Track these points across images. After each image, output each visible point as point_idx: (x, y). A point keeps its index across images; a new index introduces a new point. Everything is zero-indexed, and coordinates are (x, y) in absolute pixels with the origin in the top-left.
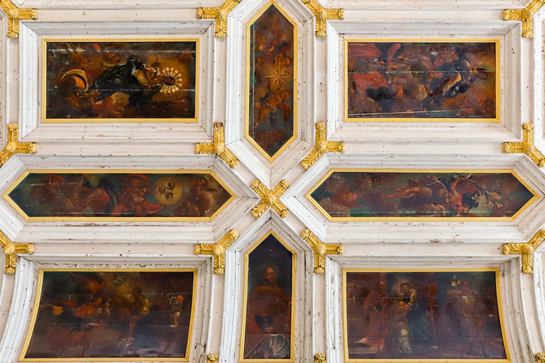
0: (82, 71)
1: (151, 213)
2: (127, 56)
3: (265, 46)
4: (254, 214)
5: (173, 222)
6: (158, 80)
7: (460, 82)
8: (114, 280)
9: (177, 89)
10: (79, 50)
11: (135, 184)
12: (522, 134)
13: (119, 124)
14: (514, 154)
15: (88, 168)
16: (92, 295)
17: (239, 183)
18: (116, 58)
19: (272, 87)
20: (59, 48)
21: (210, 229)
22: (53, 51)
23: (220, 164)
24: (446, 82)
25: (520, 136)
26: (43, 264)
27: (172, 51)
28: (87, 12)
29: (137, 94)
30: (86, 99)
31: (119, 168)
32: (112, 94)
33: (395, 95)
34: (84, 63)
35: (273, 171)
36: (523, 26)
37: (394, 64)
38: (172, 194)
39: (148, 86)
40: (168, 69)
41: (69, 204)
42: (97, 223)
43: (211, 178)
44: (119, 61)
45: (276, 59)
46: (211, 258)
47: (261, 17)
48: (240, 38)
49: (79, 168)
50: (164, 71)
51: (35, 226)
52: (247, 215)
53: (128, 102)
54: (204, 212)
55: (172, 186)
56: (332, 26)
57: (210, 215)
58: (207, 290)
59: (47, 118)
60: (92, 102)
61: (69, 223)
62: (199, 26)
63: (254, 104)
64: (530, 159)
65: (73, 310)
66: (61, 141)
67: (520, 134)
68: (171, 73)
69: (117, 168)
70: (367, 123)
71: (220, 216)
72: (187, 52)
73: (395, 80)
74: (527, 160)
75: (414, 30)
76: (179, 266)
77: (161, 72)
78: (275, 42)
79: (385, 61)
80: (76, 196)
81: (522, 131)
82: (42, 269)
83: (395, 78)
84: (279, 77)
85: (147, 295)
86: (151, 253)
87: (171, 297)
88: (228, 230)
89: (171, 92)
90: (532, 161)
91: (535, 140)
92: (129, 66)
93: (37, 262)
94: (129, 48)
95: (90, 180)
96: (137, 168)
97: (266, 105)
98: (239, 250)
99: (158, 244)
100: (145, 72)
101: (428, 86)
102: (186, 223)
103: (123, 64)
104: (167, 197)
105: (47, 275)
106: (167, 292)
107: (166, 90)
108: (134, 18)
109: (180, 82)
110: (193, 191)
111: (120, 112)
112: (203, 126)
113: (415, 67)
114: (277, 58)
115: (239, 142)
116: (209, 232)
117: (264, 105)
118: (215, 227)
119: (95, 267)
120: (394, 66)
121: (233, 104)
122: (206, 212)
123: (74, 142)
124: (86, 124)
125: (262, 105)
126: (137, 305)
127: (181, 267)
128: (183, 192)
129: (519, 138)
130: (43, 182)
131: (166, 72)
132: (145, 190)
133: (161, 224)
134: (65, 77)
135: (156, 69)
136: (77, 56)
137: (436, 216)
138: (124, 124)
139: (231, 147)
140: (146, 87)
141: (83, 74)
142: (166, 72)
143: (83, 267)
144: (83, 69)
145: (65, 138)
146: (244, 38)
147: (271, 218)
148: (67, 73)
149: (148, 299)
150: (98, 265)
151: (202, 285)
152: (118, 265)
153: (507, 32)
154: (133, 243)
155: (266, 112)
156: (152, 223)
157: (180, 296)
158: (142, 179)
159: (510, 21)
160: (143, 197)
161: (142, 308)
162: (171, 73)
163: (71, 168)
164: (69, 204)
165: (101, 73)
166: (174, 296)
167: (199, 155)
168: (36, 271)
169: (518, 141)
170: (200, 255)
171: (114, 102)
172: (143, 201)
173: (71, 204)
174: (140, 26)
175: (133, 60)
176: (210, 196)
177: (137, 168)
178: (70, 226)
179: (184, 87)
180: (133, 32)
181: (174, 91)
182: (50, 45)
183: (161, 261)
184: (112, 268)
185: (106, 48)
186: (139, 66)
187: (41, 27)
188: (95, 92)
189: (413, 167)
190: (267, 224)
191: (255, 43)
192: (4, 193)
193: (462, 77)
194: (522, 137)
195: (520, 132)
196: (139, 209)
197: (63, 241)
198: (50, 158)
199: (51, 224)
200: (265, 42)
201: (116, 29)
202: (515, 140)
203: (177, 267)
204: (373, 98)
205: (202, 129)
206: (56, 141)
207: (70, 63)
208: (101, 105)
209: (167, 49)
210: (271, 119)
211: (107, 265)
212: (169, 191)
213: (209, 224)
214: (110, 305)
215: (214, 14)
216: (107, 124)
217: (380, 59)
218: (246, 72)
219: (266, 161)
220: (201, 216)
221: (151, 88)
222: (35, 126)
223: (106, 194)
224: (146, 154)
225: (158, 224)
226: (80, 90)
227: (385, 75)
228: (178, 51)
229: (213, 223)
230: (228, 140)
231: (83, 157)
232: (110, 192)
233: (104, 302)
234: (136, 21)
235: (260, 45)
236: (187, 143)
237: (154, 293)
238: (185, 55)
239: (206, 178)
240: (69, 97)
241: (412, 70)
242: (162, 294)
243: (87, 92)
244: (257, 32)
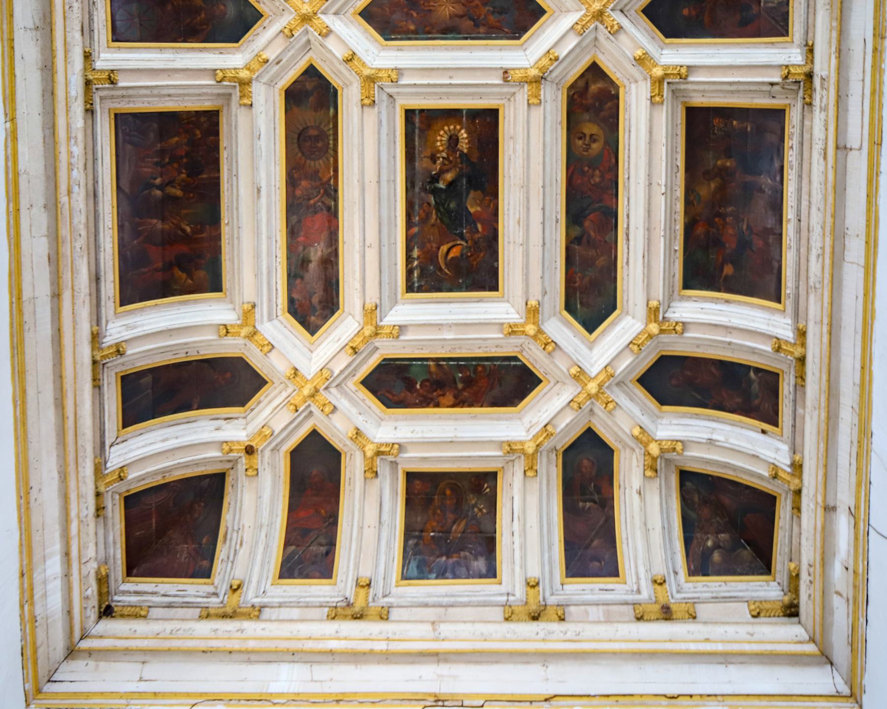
0: (441, 250)
1: (613, 161)
2: (423, 194)
3: (410, 22)
4: (616, 31)
5: (624, 133)
6: (452, 155)
9: (463, 131)
10: (416, 253)
11: (579, 181)
13: (506, 202)
15: (558, 239)
16: (711, 229)
17: (578, 50)
18: (425, 208)
19: (461, 13)
20: (413, 278)
21: (633, 86)
22: (416, 285)
23: (554, 75)
26: (673, 292)
27: (417, 139)
28: (368, 243)
29: (469, 182)
30: (476, 243)
31: (559, 200)
32: (470, 212)
34: (432, 247)
35: (564, 9)
38: (592, 135)
39: (459, 168)
40: (439, 144)
41: (601, 262)
42: (625, 226)
43: (572, 87)
44: (429, 204)
45: (426, 8)
46: (668, 83)
47: (375, 28)
48: (400, 54)
49: (558, 249)
50: (441, 148)
51: (627, 301)
52: (616, 39)
53: (479, 192)
54: (614, 95)
55: (581, 135)
57: (617, 88)
58: (706, 87)
59: (497, 290)
60: (479, 235)
61: (625, 260)
62: (385, 104)
63: (482, 34)
65: (728, 251)
66: (525, 271)
68: (443, 139)
69: (559, 203)
71: (618, 75)
72: (417, 120)
77: (443, 151)
78: (405, 10)
80: (592, 253)
84: (448, 5)
85: (712, 163)
87: (715, 134)
88: (634, 63)
89: (466, 138)
92: (435, 192)
94: (413, 192)
95: (573, 236)
96: (559, 180)
97: (483, 19)
98: (660, 50)
99: (650, 149)
100: (442, 172)
102: (627, 117)
103: (433, 199)
104: (595, 141)
105: (686, 286)
107: (464, 146)
108: (374, 185)
109: (455, 127)
110: (587, 109)
111: (490, 201)
112: (508, 97)
114: (425, 6)
115: (528, 52)
116: (637, 88)
117: (484, 22)
118: (631, 80)
119: (678, 227)
121: (480, 60)
122: (613, 92)
123: (527, 255)
124: (506, 243)
125: (484, 25)
126: (723, 174)
127: (679, 121)
128: (590, 121)
130: (576, 293)
131: (442, 145)
132: (586, 168)
133: (627, 147)
134: (448, 270)
135: (439, 158)
136: (422, 256)
138: (506, 196)
139: (533, 60)
140: (461, 169)
141: (444, 248)
142: (442, 145)
143: (677, 243)
144: (439, 248)
145: (521, 266)
146: (399, 48)
147: (622, 11)
148: (443, 267)
151: (701, 95)
152: (676, 199)
154: (649, 180)
155: (492, 19)
156: (626, 158)
158: (573, 173)
160: (594, 170)
161: (728, 168)
162: (443, 139)
163: (558, 260)
164: (601, 262)
165: (443, 226)
167: (543, 101)
168: (682, 298)
171: (479, 209)
172: (600, 171)
173: (602, 258)
174: (384, 178)
175: (428, 187)
176: (594, 88)
177: (559, 180)
178: (628, 259)
179: (460, 123)
180: (393, 186)
181: (465, 135)
182: (410, 288)
183: (672, 146)
184: (680, 207)
185: (414, 220)
186: (435, 179)
187: (387, 300)
188: (467, 232)
190: (628, 16)
191: (406, 34)
192: (588, 339)
196: (608, 176)
197: (646, 265)
198: (547, 284)
199: (625, 282)
200: (405, 23)
201: (389, 208)
205: (512, 99)
206: (524, 277)
207: (431, 265)
208: (482, 224)
209: (414, 145)
210: (500, 13)
212: (588, 138)
213: (627, 88)
215: (369, 85)
216: (506, 217)
218: (441, 46)
219: (552, 18)
220: (618, 99)
221: (461, 163)
222: (507, 305)
223: (592, 215)
224: (541, 166)
225: (627, 151)
226: (465, 251)
228: (417, 131)
229: (626, 82)
230: (525, 64)
231: (544, 244)
232: (587, 212)
233: (719, 215)
234: (379, 182)
235: (409, 29)
236: (528, 115)
237: (711, 155)
238: (421, 122)
239: (572, 93)
240: (473, 265)
243: (467, 242)
244: (393, 33)
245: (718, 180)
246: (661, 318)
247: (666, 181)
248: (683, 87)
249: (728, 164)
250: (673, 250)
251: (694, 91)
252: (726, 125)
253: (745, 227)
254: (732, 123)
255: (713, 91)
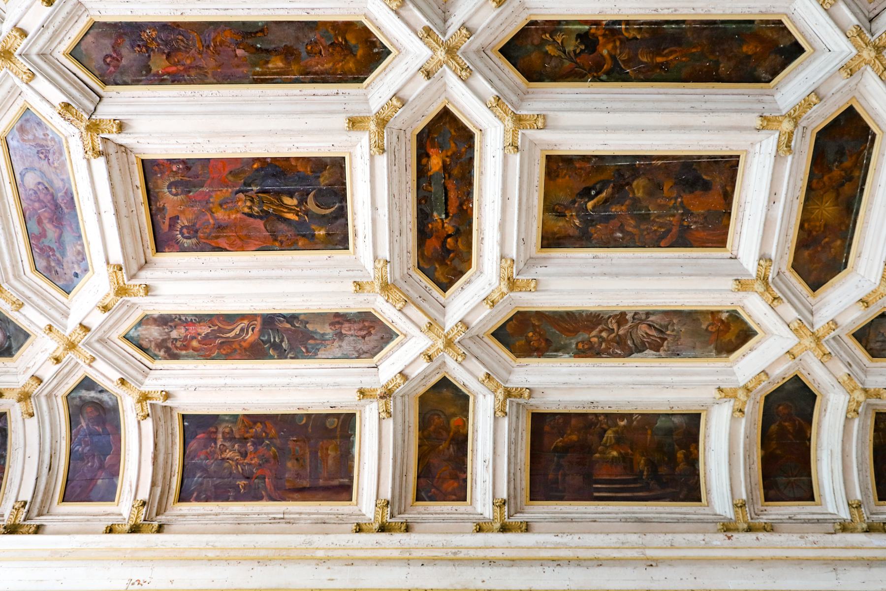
7: (589, 201)
12: (519, 140)
14: (531, 113)
24: (606, 201)
25: (522, 137)
33: (675, 184)
36: (513, 273)
37: (672, 221)
56: (747, 270)
64: (509, 106)
67: (522, 140)
70: (716, 149)
73: (673, 202)
74: (512, 104)
75: (644, 265)
79: (682, 225)
81: (519, 144)
83: (671, 205)
90: (507, 103)
91: (502, 132)
101: (631, 196)
113: (645, 218)
120: (671, 219)
129: (523, 134)
137: (635, 22)
153: (531, 262)
159: (528, 278)
169: (524, 131)
189: (662, 91)
193: (586, 207)
194: (519, 136)
195: (522, 143)
202: (528, 132)
204: (703, 179)
217: (689, 227)
227: (684, 208)
241: (649, 214)
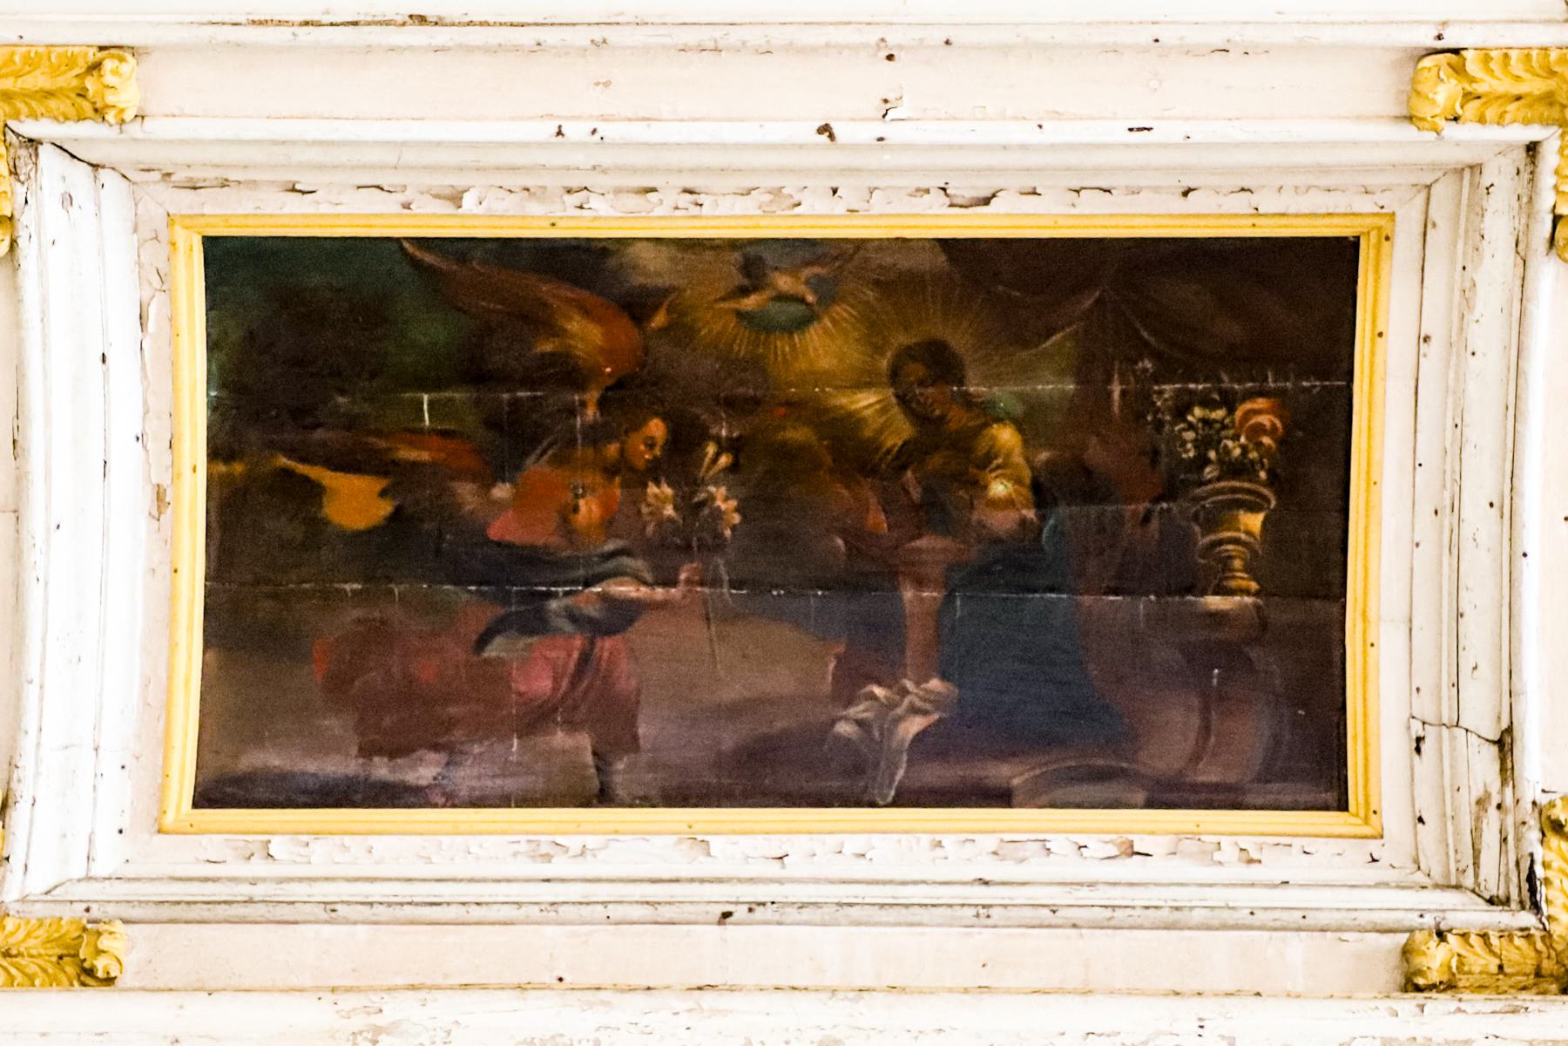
8: (744, 292)
16: (593, 396)
46: (1532, 149)
65: (466, 493)
76: (1254, 199)
82: (189, 220)
85: (1004, 394)
86: (1057, 115)
93: (156, 176)
106: (1158, 378)
149: (1019, 425)
150: (618, 191)
152: (777, 192)
157: (1261, 403)
166: (1207, 403)
170: (1450, 130)
203: (1241, 203)
211: (691, 192)
214: (733, 468)
237: (1054, 386)
242: (1116, 390)
245: (900, 431)
246: (29, 128)
247: (907, 147)
248: (1499, 224)
249: (999, 488)
250: (459, 181)
251: (1467, 294)
252: (1237, 469)
253: (625, 589)
254: (1253, 508)
255: (1455, 392)
